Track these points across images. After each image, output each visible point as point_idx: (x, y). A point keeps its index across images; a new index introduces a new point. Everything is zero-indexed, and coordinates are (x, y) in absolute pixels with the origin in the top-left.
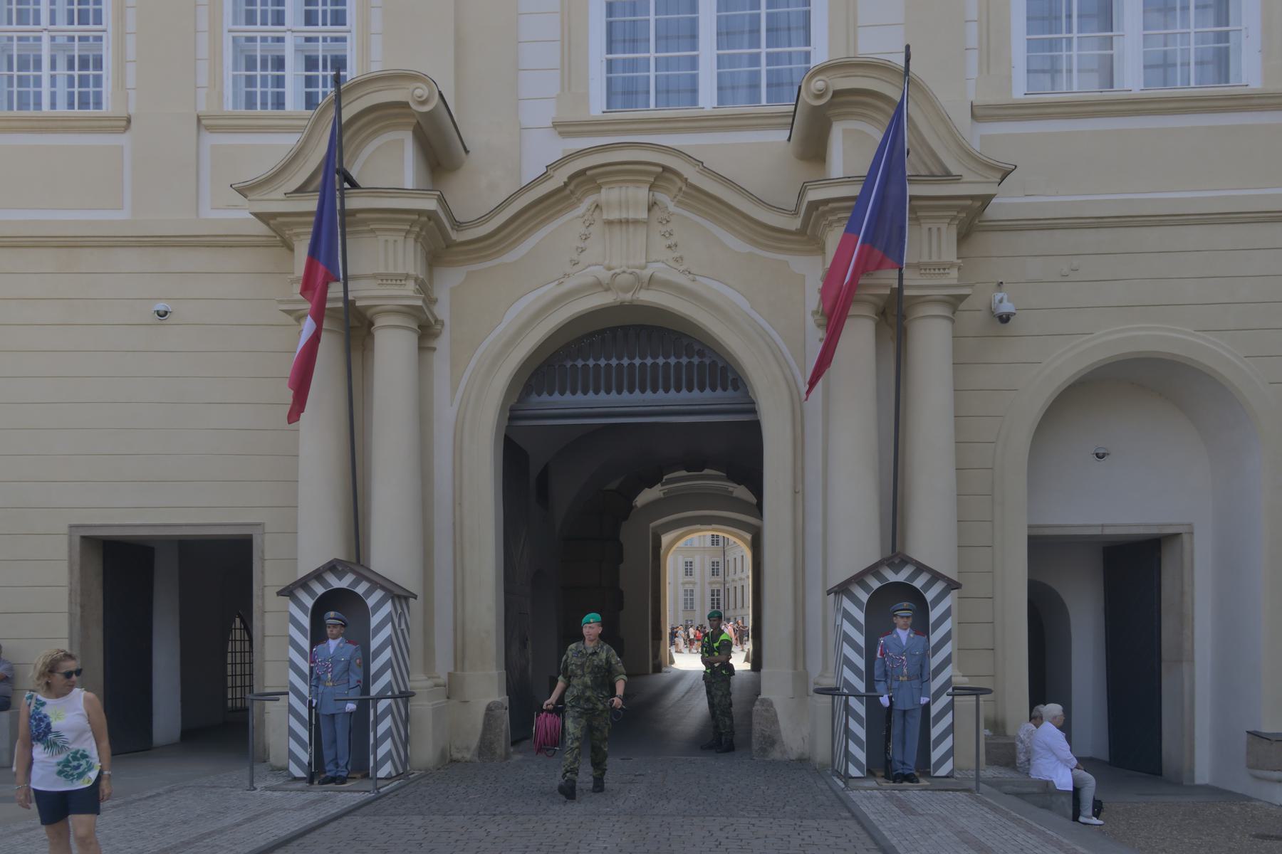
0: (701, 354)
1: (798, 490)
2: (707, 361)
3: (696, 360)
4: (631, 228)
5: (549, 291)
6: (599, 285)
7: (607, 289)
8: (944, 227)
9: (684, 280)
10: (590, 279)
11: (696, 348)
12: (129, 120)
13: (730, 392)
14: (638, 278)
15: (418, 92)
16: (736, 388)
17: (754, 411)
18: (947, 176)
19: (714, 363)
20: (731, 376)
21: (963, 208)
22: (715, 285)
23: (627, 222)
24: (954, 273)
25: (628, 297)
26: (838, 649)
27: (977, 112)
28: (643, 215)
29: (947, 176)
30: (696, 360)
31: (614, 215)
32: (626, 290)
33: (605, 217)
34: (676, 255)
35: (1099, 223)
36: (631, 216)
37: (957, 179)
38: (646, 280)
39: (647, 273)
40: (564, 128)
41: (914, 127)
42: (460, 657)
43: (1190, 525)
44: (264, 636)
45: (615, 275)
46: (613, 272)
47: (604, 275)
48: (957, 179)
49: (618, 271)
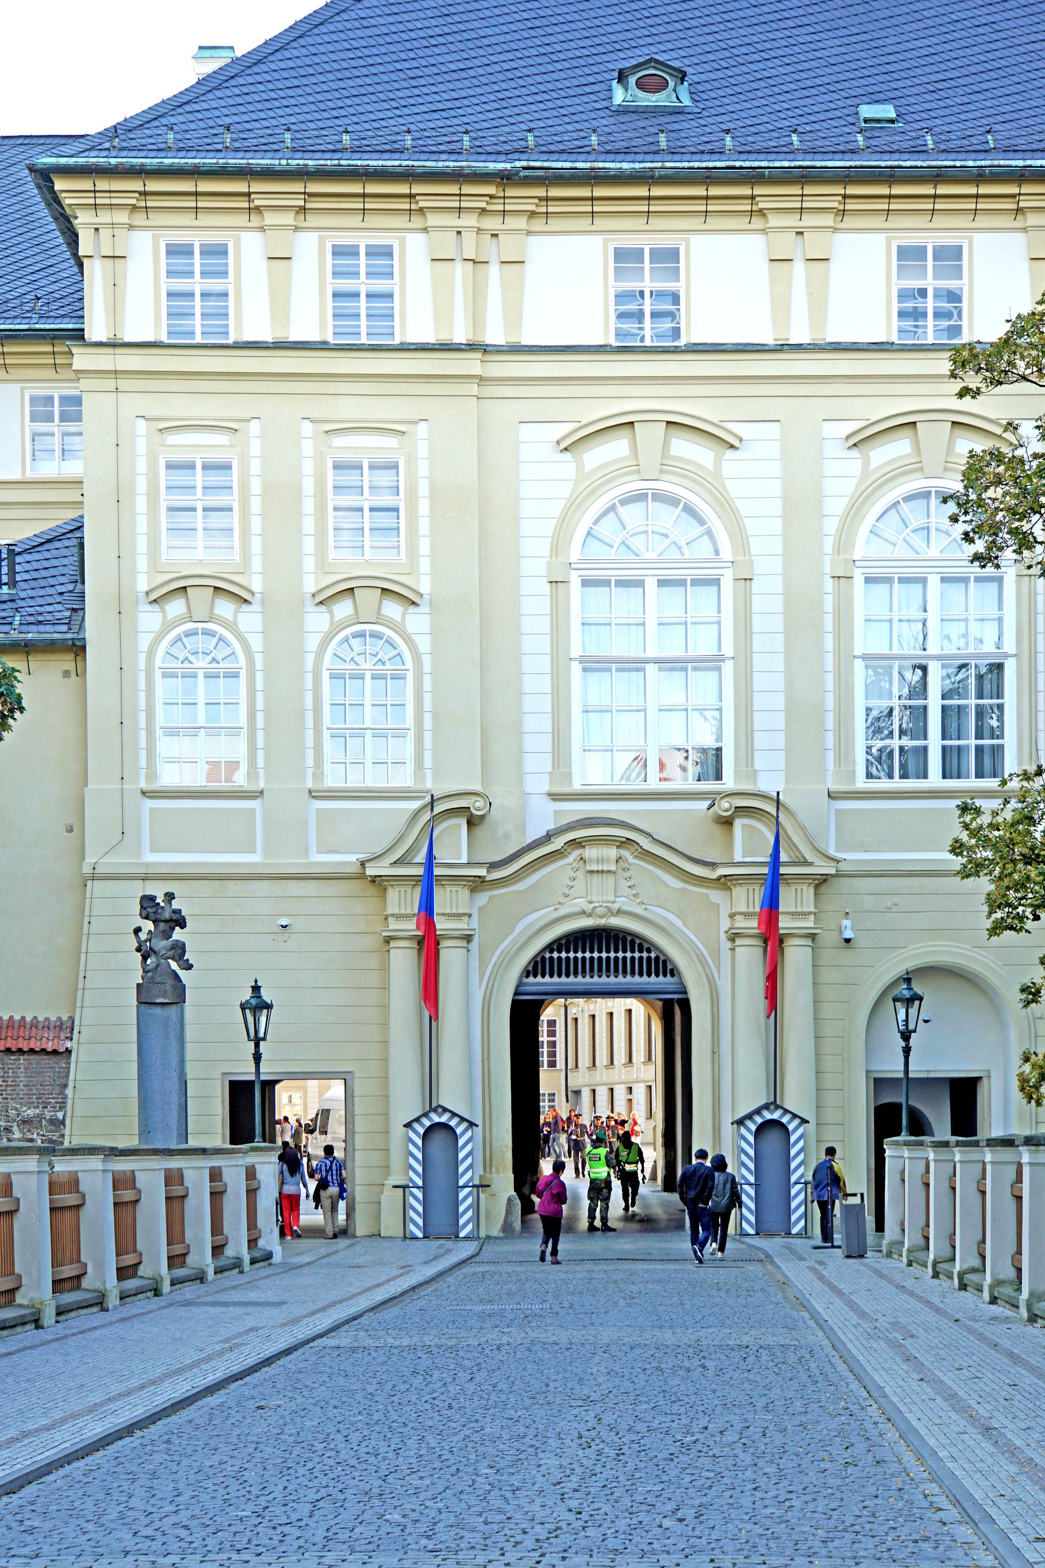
0: (649, 951)
1: (715, 1053)
2: (653, 955)
3: (645, 955)
4: (605, 875)
5: (547, 914)
6: (583, 913)
7: (590, 915)
8: (805, 888)
9: (639, 910)
10: (577, 909)
11: (646, 946)
12: (262, 792)
13: (669, 978)
14: (610, 910)
15: (478, 804)
16: (673, 975)
17: (685, 993)
18: (805, 863)
19: (657, 958)
20: (669, 967)
21: (815, 879)
22: (660, 911)
23: (603, 871)
24: (812, 917)
25: (602, 922)
26: (739, 1157)
27: (832, 795)
28: (613, 868)
29: (805, 863)
30: (645, 955)
31: (594, 868)
32: (602, 917)
33: (588, 868)
34: (634, 892)
35: (911, 874)
36: (605, 868)
37: (811, 864)
38: (615, 911)
39: (615, 907)
40: (555, 797)
41: (784, 830)
42: (488, 1164)
43: (988, 1071)
44: (354, 1150)
45: (595, 907)
46: (593, 905)
47: (588, 908)
48: (811, 864)
49: (596, 905)
